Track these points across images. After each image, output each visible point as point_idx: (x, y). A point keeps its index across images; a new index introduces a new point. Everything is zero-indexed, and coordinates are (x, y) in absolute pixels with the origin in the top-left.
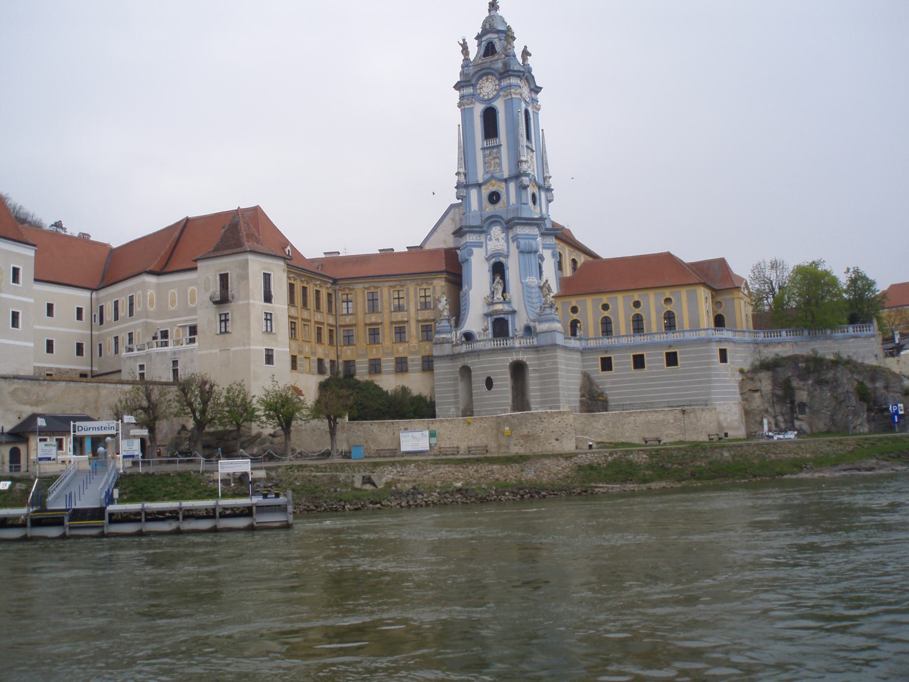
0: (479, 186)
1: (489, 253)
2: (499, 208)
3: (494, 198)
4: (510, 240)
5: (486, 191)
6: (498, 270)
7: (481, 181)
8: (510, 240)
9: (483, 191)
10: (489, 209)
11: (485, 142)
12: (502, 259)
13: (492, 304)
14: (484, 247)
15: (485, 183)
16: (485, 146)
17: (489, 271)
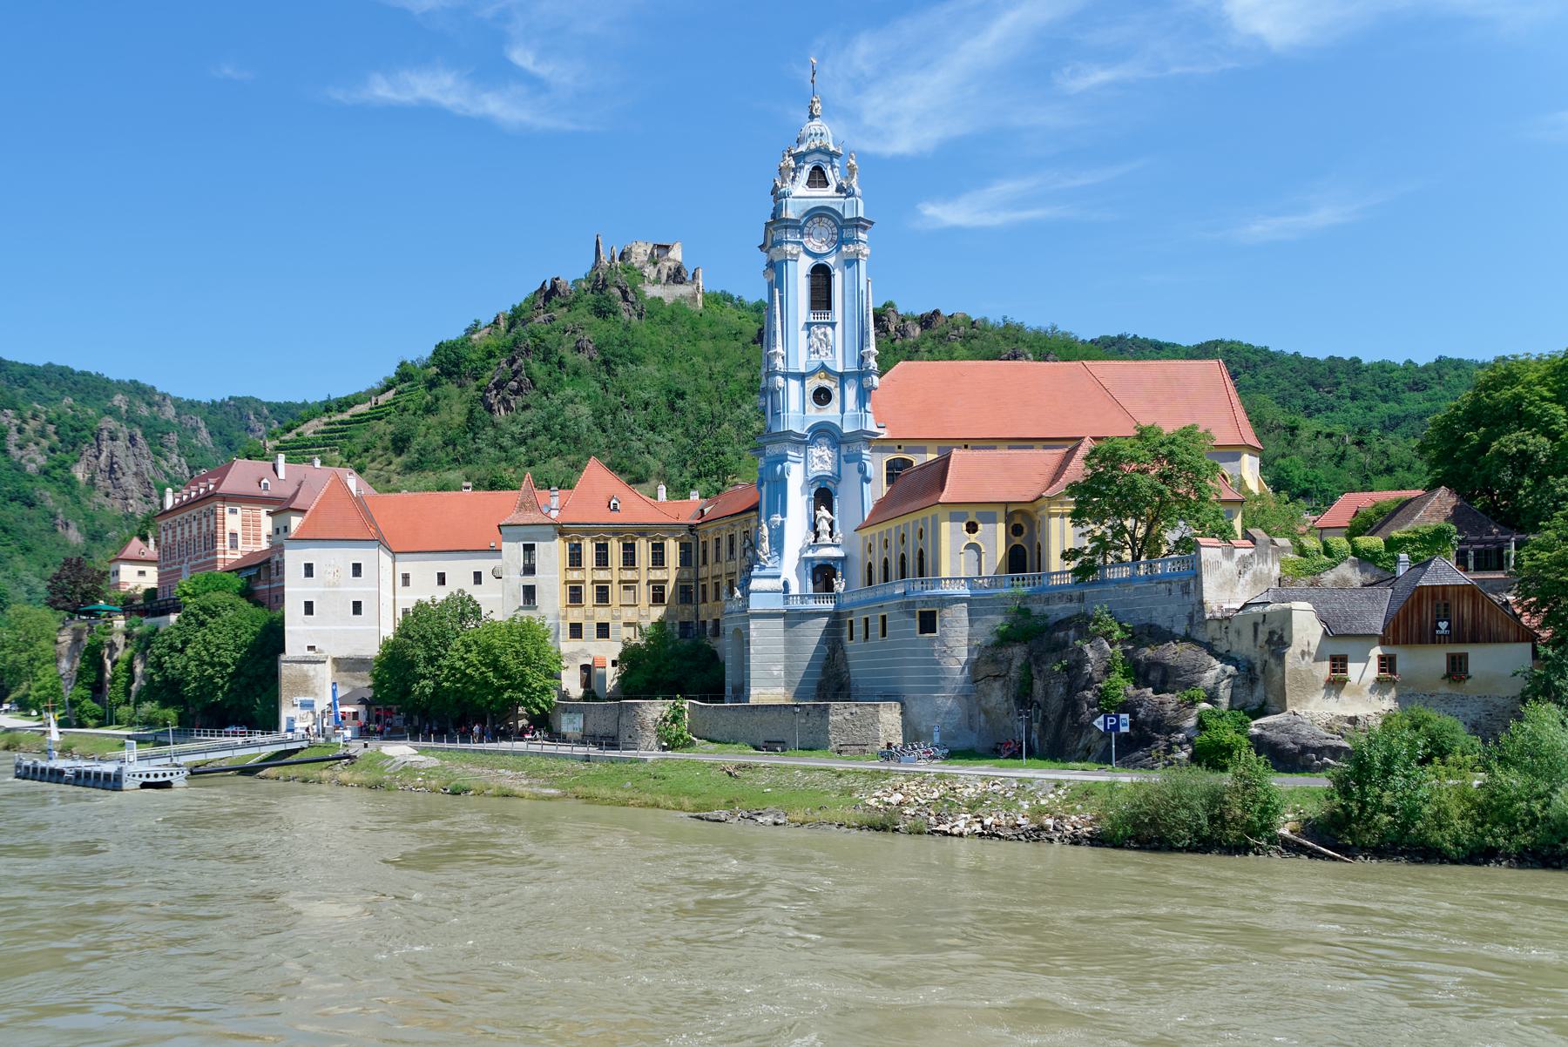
0: (802, 377)
1: (811, 476)
2: (831, 412)
3: (822, 396)
4: (842, 458)
5: (812, 384)
6: (823, 496)
8: (842, 458)
9: (807, 386)
10: (816, 414)
11: (812, 315)
12: (830, 485)
13: (815, 545)
14: (802, 464)
15: (813, 373)
16: (812, 320)
17: (809, 499)
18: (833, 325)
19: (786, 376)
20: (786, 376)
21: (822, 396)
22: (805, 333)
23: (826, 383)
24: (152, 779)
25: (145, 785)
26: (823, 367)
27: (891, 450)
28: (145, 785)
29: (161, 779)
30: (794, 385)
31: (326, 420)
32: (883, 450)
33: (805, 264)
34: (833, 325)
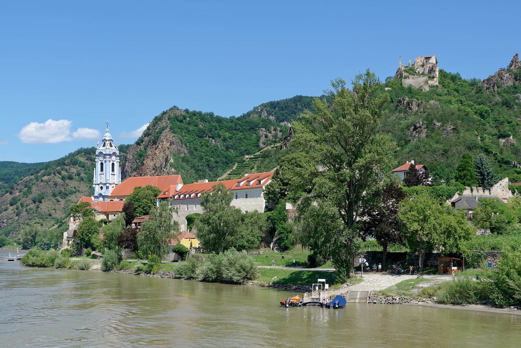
0: (98, 184)
3: (102, 188)
7: (99, 183)
15: (100, 184)
18: (103, 174)
19: (96, 184)
20: (96, 184)
21: (102, 188)
22: (99, 176)
23: (102, 186)
24: (10, 259)
25: (9, 260)
26: (101, 183)
27: (110, 198)
28: (9, 260)
29: (12, 259)
30: (97, 186)
31: (272, 146)
32: (109, 198)
33: (100, 162)
34: (103, 174)
